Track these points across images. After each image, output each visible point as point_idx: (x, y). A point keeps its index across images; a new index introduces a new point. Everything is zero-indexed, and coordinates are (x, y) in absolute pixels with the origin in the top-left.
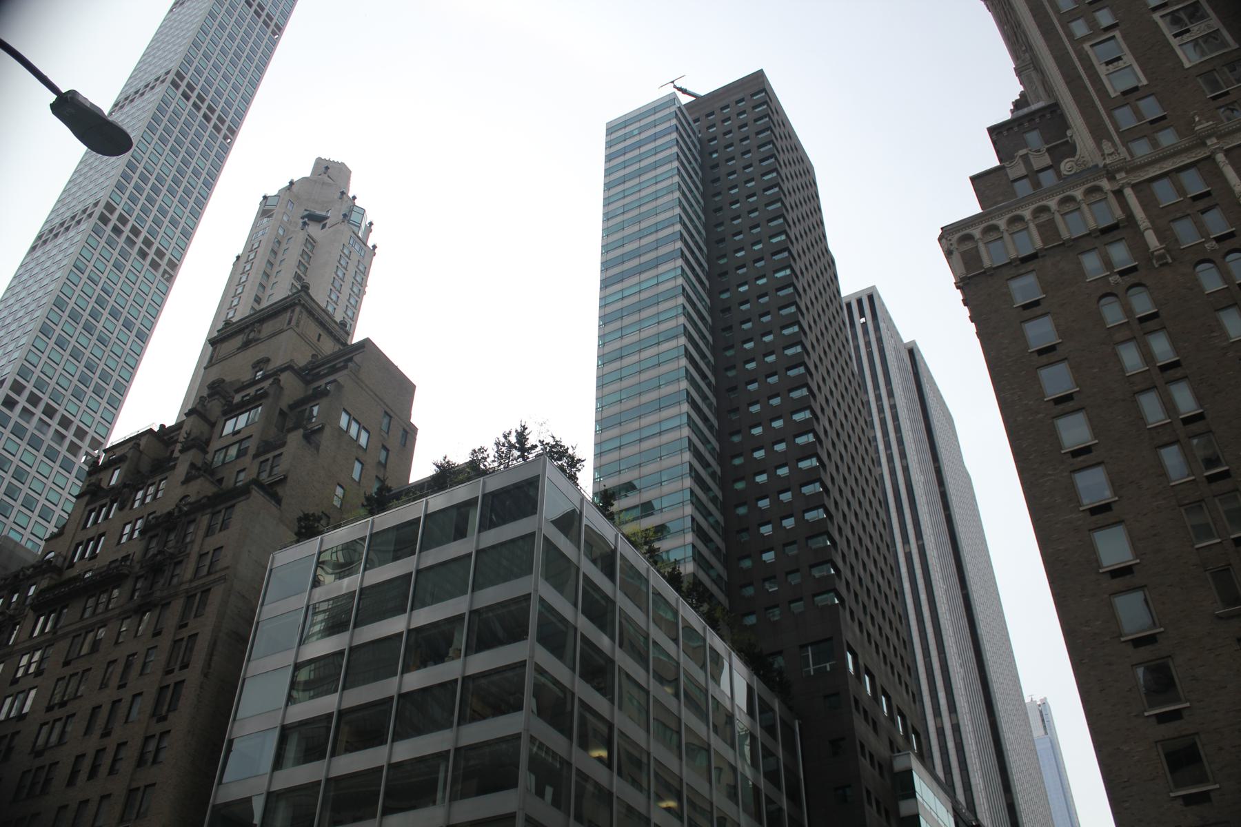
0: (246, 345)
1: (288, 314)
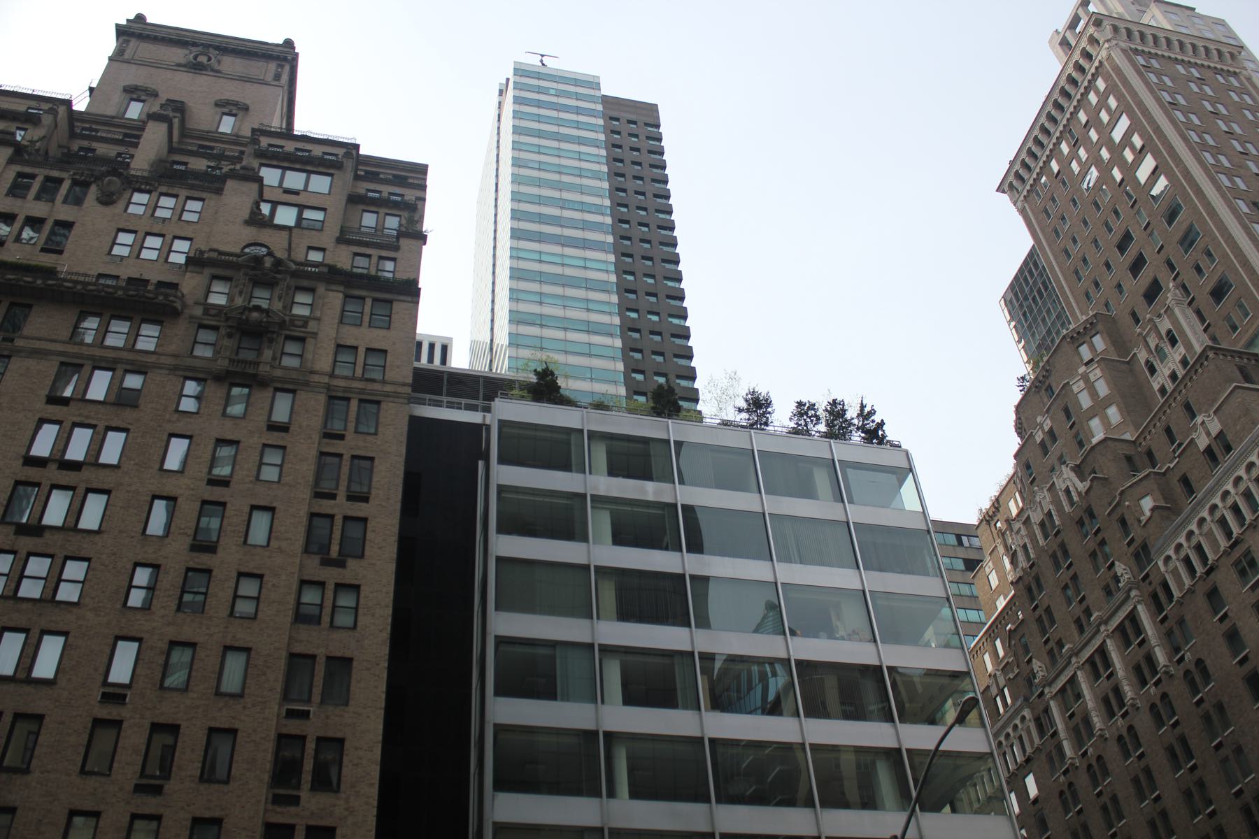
0: (196, 67)
1: (272, 66)
